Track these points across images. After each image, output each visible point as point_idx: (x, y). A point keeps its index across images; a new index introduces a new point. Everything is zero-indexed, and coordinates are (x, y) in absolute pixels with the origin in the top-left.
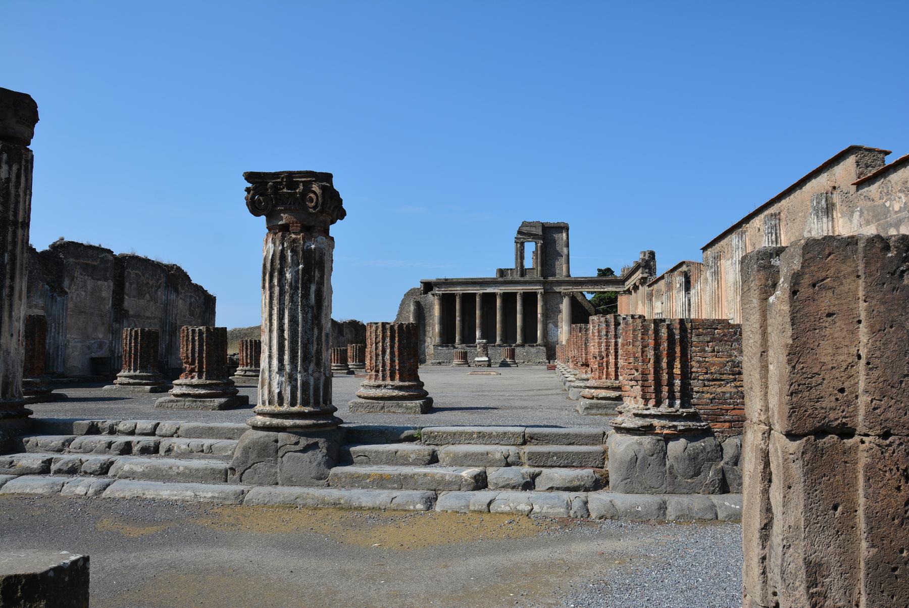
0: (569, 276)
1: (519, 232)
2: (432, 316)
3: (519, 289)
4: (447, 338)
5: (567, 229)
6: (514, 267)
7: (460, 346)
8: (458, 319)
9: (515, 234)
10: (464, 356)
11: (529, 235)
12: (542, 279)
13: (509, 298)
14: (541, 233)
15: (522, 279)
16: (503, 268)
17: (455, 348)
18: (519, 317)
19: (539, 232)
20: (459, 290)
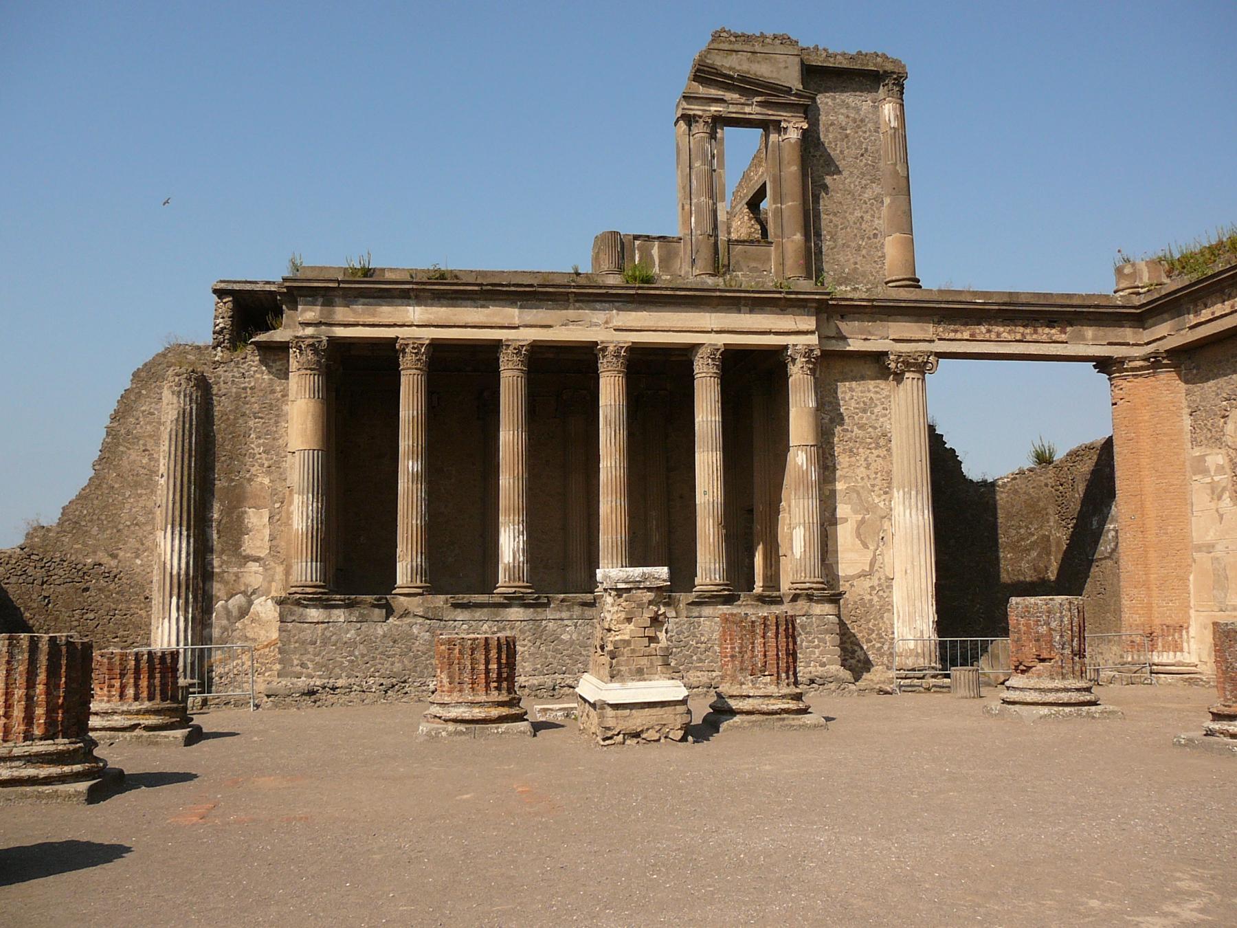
0: (915, 283)
1: (704, 74)
2: (276, 452)
3: (708, 331)
4: (352, 561)
5: (902, 87)
6: (675, 231)
7: (415, 605)
8: (409, 466)
9: (682, 80)
10: (501, 665)
11: (747, 86)
12: (806, 285)
13: (659, 378)
14: (797, 85)
15: (720, 282)
16: (628, 229)
17: (390, 611)
18: (707, 464)
19: (791, 78)
20: (416, 324)
